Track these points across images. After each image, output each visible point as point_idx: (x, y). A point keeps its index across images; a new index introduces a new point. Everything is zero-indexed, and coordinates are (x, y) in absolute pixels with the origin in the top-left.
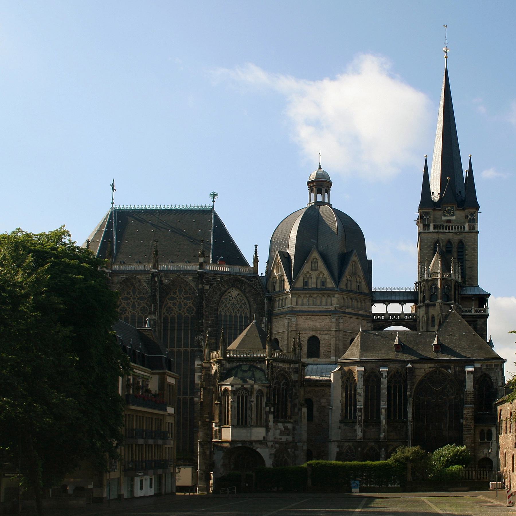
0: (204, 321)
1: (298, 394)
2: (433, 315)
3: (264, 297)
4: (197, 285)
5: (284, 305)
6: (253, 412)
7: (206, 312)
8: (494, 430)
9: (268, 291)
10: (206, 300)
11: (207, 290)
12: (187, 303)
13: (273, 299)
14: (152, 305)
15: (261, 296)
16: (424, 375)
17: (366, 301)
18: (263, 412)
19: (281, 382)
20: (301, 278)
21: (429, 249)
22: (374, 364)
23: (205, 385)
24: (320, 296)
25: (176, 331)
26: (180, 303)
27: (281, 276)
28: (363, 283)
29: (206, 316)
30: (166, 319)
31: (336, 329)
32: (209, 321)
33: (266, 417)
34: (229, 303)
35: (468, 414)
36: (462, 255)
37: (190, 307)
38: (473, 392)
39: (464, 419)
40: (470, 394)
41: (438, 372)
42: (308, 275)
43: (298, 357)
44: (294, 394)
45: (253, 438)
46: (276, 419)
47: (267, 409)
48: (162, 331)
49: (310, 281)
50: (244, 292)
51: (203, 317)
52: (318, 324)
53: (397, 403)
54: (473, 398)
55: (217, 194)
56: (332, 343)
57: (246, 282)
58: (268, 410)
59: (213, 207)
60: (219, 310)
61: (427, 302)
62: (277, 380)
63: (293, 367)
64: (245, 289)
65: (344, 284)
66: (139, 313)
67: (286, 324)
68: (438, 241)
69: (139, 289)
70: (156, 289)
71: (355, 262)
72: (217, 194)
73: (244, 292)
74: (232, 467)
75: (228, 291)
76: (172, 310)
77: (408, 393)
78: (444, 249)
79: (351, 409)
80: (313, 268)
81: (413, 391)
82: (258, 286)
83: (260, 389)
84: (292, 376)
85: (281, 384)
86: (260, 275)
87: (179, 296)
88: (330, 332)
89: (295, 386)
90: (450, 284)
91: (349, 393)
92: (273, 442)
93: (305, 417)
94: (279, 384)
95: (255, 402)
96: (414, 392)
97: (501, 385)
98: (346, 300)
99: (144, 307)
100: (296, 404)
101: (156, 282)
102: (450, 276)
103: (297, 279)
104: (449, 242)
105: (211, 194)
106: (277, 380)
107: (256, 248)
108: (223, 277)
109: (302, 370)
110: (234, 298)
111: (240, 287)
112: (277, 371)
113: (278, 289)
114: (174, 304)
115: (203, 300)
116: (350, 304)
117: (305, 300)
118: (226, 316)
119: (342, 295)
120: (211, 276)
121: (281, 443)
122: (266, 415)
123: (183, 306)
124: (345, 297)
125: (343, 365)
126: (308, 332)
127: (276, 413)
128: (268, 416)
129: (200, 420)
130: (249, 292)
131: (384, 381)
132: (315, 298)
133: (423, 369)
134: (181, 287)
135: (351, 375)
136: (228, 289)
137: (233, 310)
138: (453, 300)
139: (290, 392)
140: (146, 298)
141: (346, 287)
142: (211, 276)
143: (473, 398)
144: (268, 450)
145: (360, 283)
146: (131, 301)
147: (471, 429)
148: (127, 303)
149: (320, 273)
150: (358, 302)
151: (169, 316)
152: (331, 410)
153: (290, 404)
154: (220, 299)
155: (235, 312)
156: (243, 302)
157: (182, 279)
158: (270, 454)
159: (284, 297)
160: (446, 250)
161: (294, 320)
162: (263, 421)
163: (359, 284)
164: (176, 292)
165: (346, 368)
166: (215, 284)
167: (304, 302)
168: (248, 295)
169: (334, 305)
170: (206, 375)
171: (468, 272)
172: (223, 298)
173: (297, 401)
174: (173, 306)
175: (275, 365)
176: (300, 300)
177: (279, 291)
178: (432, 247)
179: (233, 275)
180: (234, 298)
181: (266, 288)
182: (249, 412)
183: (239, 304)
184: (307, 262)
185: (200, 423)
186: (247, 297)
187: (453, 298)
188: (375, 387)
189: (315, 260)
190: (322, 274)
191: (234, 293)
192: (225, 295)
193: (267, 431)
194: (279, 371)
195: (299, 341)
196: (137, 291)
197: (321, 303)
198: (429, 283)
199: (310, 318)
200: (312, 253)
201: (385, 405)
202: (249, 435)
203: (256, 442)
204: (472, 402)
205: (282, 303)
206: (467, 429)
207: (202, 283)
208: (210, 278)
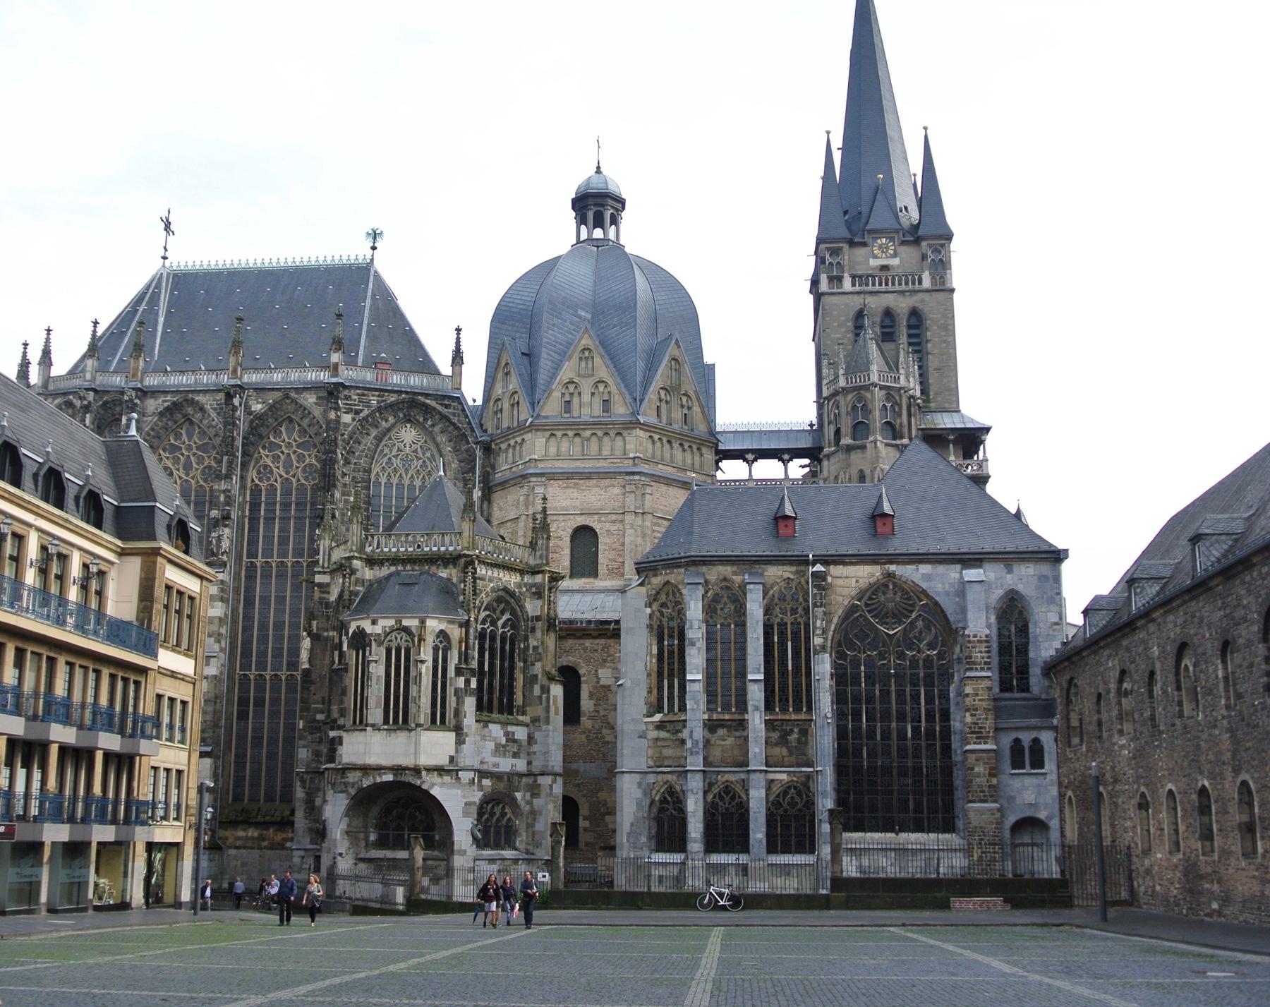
0: (337, 495)
1: (540, 650)
2: (861, 471)
3: (477, 443)
4: (325, 413)
5: (517, 459)
6: (423, 688)
7: (344, 475)
8: (1047, 738)
9: (485, 431)
10: (345, 448)
11: (346, 425)
12: (304, 456)
13: (493, 446)
14: (225, 458)
15: (468, 443)
16: (854, 593)
17: (704, 450)
18: (450, 691)
19: (499, 619)
20: (557, 394)
21: (843, 330)
22: (729, 568)
23: (317, 629)
24: (600, 433)
25: (277, 521)
26: (289, 455)
27: (513, 393)
28: (696, 409)
29: (345, 485)
30: (256, 491)
31: (636, 508)
32: (348, 495)
33: (458, 703)
34: (396, 457)
35: (977, 695)
36: (918, 344)
37: (311, 465)
38: (987, 636)
39: (968, 710)
40: (979, 642)
41: (891, 587)
42: (571, 388)
43: (541, 557)
44: (531, 651)
45: (424, 761)
46: (485, 713)
47: (461, 682)
48: (247, 520)
49: (576, 400)
50: (431, 432)
51: (335, 486)
52: (594, 498)
53: (790, 668)
54: (988, 652)
55: (381, 233)
56: (627, 541)
57: (435, 409)
58: (462, 686)
59: (372, 260)
60: (374, 473)
61: (847, 440)
62: (488, 613)
63: (530, 581)
64: (433, 426)
65: (654, 407)
66: (198, 482)
67: (522, 498)
68: (860, 315)
69: (199, 427)
70: (234, 424)
71: (676, 360)
72: (381, 233)
73: (431, 432)
74: (373, 837)
75: (396, 430)
76: (271, 472)
77: (818, 641)
78: (878, 330)
79: (671, 687)
80: (582, 372)
81: (830, 638)
82: (462, 418)
83: (442, 631)
84: (527, 605)
85: (500, 623)
86: (471, 403)
87: (287, 440)
88: (621, 516)
89: (533, 630)
90: (897, 398)
91: (666, 643)
92: (475, 770)
93: (557, 709)
94: (494, 623)
95: (430, 663)
96: (832, 640)
97: (1057, 620)
98: (659, 444)
99: (210, 467)
100: (536, 676)
101: (235, 409)
102: (897, 380)
103: (548, 397)
104: (888, 313)
105: (368, 234)
106: (488, 613)
107: (458, 334)
108: (383, 396)
109: (550, 589)
110: (408, 446)
111: (421, 420)
112: (488, 589)
113: (505, 425)
114: (276, 459)
115: (336, 444)
116: (667, 456)
117: (565, 444)
118: (389, 485)
119: (650, 431)
120: (358, 395)
121: (496, 776)
122: (458, 699)
123: (295, 463)
124: (656, 437)
125: (651, 573)
126: (572, 517)
127: (485, 698)
128: (463, 702)
129: (301, 718)
130: (442, 432)
131: (755, 608)
132: (588, 439)
133: (854, 580)
134: (291, 420)
135: (671, 596)
136: (393, 426)
137: (407, 471)
138: (906, 436)
139: (522, 646)
140: (214, 447)
141: (659, 415)
142: (358, 395)
143: (988, 652)
144: (459, 791)
145: (689, 408)
146: (183, 454)
147: (988, 737)
148: (173, 458)
149: (599, 382)
150: (684, 451)
151: (263, 486)
152: (621, 688)
153: (522, 676)
154: (378, 446)
155: (409, 476)
156: (428, 454)
157: (294, 401)
158: (466, 804)
159: (519, 439)
160: (883, 334)
161: (539, 490)
162: (450, 714)
163: (686, 412)
164: (281, 432)
165: (657, 581)
166: (366, 412)
167: (563, 449)
168: (438, 439)
169: (632, 455)
170: (320, 603)
171: (933, 379)
172: (383, 443)
173: (538, 668)
174: (273, 463)
175: (484, 572)
176: (553, 439)
177: (509, 428)
178: (850, 324)
179: (407, 393)
180: (408, 446)
181: (481, 425)
182: (413, 691)
183: (419, 459)
184: (570, 357)
185: (301, 724)
186: (437, 445)
187: (906, 430)
188: (732, 626)
189: (587, 353)
190: (604, 385)
191: (408, 435)
192: (387, 438)
193: (460, 741)
194: (493, 590)
195: (545, 519)
196: (197, 430)
197: (600, 450)
198: (850, 397)
199: (575, 484)
200: (582, 338)
201: (759, 673)
202: (412, 750)
203: (430, 770)
204: (986, 663)
205: (513, 455)
206: (977, 738)
207: (337, 409)
208: (355, 397)
